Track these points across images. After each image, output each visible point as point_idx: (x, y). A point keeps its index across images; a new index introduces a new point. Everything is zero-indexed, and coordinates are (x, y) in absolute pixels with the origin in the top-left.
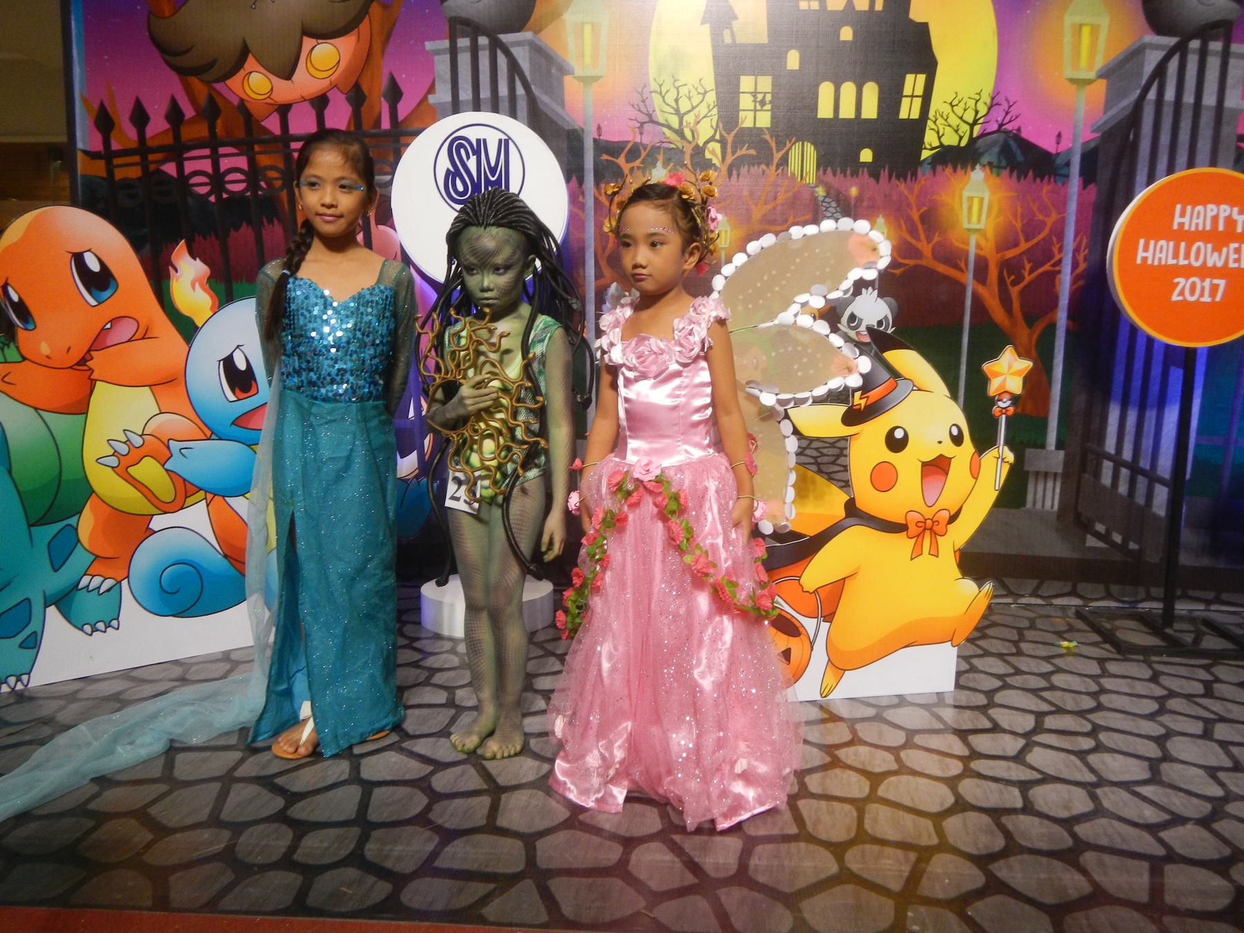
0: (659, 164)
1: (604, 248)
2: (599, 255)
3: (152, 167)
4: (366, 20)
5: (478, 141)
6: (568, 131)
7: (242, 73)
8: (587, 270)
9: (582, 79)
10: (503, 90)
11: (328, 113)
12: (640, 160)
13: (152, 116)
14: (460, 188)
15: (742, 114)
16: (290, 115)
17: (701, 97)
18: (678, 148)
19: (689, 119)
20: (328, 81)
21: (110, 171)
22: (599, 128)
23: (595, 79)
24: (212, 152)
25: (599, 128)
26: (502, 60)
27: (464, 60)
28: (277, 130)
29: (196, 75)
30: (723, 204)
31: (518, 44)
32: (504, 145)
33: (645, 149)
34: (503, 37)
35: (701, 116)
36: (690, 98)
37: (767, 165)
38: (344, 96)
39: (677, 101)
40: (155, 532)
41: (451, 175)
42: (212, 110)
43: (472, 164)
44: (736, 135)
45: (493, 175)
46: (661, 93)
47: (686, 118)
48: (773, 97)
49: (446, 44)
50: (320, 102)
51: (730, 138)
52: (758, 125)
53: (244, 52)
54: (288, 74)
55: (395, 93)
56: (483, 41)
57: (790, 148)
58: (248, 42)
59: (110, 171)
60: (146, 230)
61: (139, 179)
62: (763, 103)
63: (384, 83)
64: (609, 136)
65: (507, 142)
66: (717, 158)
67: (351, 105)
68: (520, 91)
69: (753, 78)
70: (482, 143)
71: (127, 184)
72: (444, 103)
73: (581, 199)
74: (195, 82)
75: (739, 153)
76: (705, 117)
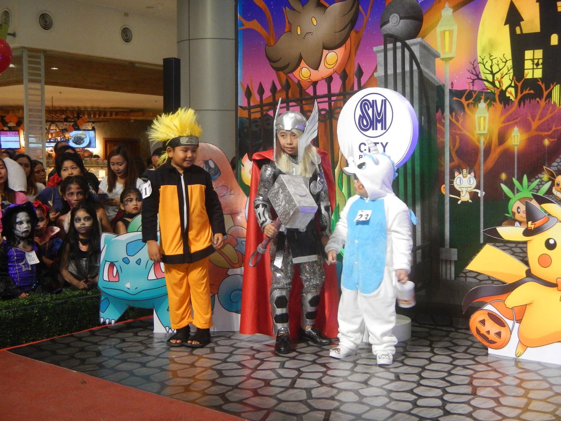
0: (482, 101)
1: (454, 146)
2: (451, 149)
3: (265, 113)
4: (349, 40)
5: (373, 101)
6: (438, 87)
7: (299, 68)
8: (445, 158)
9: (444, 59)
10: (407, 68)
11: (331, 84)
12: (473, 99)
13: (265, 90)
14: (365, 123)
15: (526, 71)
16: (317, 86)
17: (504, 63)
18: (492, 92)
19: (498, 76)
20: (332, 70)
21: (250, 116)
22: (452, 84)
23: (450, 59)
24: (286, 105)
25: (452, 84)
26: (407, 53)
27: (390, 54)
28: (312, 94)
29: (282, 71)
30: (515, 121)
31: (415, 44)
32: (384, 102)
33: (475, 94)
34: (408, 42)
35: (504, 74)
36: (498, 65)
37: (540, 99)
38: (339, 76)
39: (491, 67)
40: (229, 276)
41: (362, 118)
42: (287, 86)
43: (370, 112)
44: (523, 83)
45: (379, 118)
46: (483, 64)
47: (496, 76)
48: (543, 61)
49: (382, 47)
50: (329, 79)
51: (519, 85)
52: (535, 77)
53: (301, 58)
54: (317, 68)
55: (360, 73)
56: (399, 44)
57: (553, 88)
58: (302, 55)
59: (250, 116)
60: (261, 141)
61: (260, 118)
62: (537, 64)
63: (356, 69)
64: (457, 88)
65: (385, 101)
66: (513, 96)
67: (342, 80)
68: (415, 67)
69: (532, 51)
70: (375, 102)
71: (255, 121)
72: (381, 76)
73: (443, 121)
74: (281, 73)
75: (525, 93)
76: (506, 74)
